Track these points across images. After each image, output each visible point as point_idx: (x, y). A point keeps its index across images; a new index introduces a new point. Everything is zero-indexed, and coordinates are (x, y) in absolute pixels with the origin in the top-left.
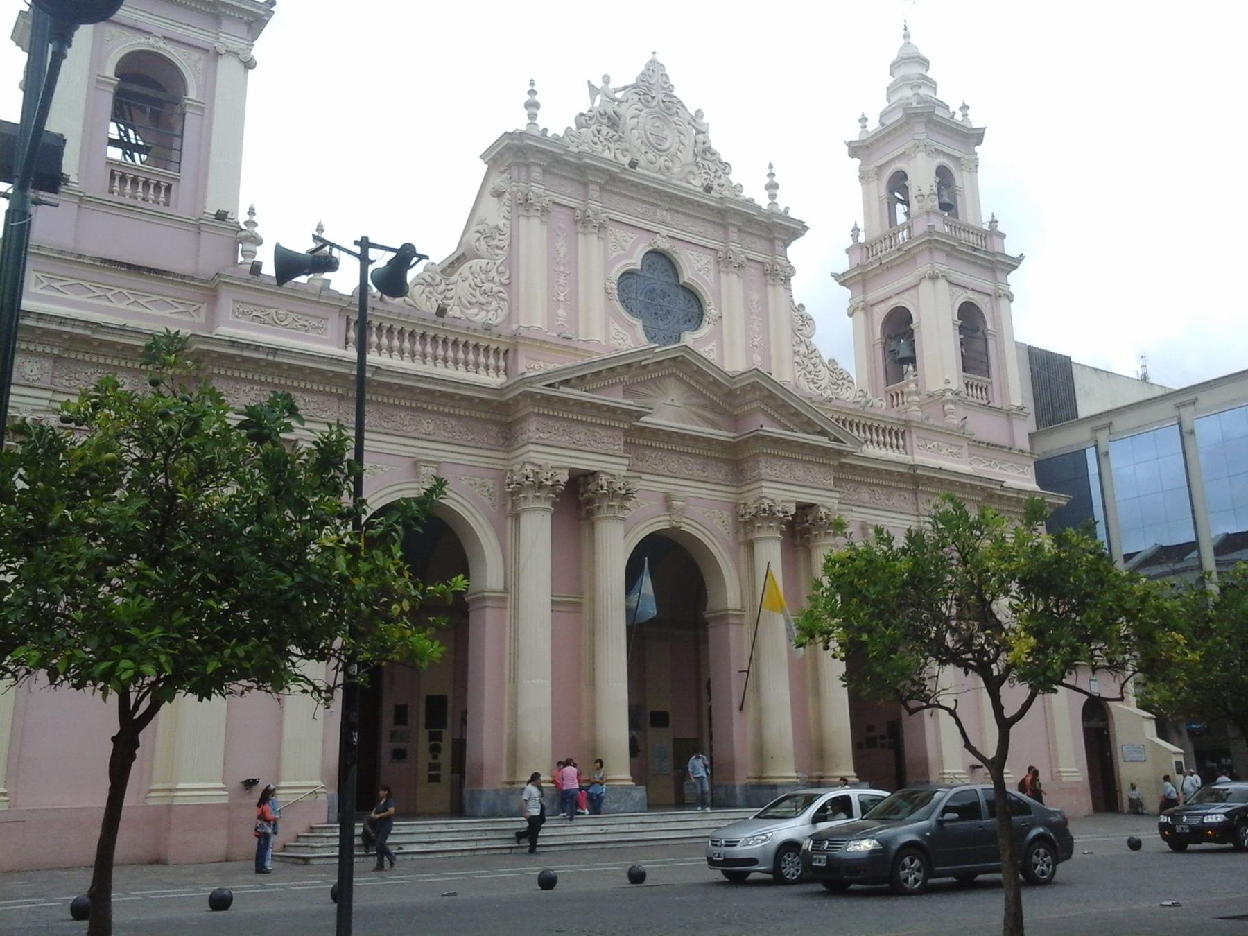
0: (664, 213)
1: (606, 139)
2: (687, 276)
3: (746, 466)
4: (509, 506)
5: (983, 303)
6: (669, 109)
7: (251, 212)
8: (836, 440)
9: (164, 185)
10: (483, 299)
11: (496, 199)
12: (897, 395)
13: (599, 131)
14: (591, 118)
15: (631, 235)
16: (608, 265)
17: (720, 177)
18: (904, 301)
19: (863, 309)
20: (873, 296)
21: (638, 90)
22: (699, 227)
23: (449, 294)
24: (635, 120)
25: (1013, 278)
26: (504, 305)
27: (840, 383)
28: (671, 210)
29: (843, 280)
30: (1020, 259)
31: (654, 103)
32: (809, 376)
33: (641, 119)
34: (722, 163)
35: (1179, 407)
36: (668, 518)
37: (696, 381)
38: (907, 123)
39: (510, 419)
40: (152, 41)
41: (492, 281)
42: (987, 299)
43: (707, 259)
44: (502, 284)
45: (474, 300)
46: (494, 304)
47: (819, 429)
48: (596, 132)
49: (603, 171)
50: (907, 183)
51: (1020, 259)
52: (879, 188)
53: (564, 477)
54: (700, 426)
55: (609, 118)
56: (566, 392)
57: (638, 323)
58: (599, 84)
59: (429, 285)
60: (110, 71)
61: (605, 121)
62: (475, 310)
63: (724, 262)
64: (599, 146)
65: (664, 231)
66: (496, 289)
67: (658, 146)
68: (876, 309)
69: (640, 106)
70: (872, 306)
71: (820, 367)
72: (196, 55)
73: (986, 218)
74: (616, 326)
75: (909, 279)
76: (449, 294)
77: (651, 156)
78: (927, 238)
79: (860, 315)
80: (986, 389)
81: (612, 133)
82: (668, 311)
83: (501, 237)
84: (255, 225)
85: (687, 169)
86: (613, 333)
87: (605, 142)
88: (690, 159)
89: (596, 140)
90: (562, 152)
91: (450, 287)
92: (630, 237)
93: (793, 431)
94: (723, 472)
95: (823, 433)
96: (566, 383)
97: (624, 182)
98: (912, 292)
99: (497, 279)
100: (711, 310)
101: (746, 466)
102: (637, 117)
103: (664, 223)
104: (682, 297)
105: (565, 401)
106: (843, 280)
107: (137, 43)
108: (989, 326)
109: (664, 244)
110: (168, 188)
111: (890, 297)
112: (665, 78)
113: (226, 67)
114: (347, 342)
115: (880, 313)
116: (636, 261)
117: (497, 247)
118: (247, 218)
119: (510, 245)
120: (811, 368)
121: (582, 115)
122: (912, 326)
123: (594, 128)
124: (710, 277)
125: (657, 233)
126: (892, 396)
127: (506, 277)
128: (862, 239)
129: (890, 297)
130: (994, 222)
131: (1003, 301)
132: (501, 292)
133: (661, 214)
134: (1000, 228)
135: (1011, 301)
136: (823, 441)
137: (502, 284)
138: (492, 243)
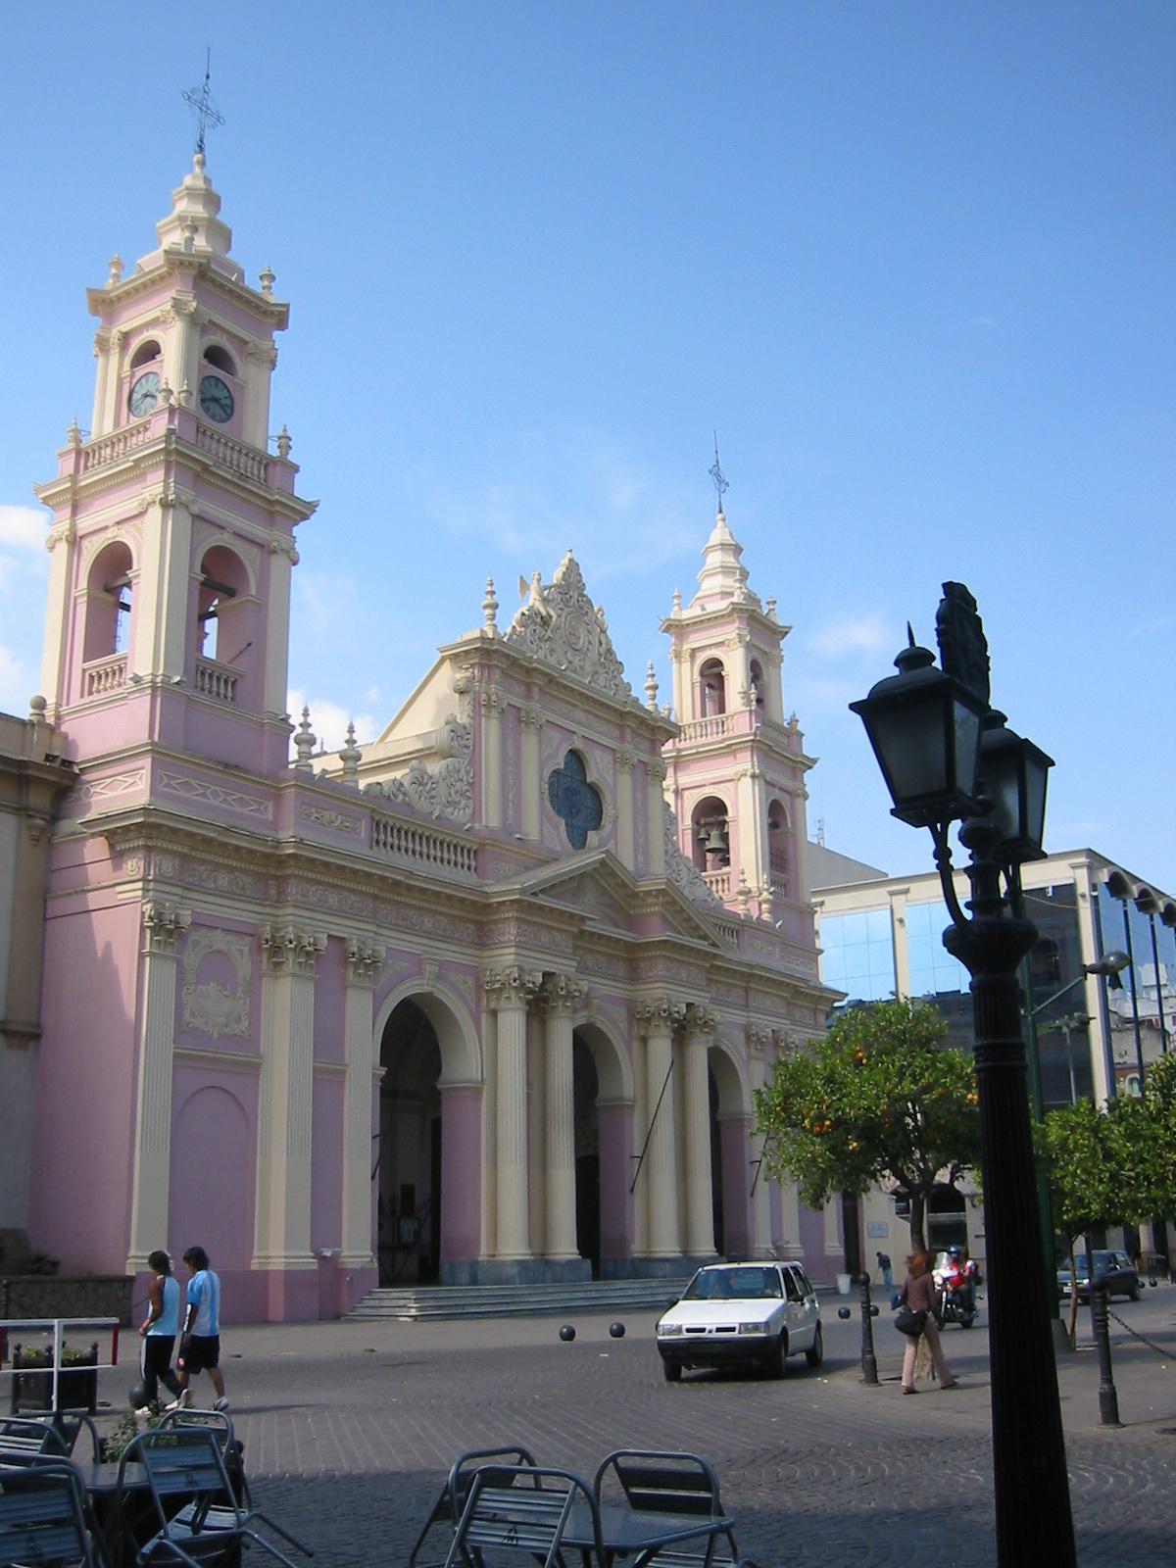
3: (642, 965)
4: (484, 1002)
5: (784, 800)
6: (581, 608)
7: (306, 714)
8: (714, 945)
10: (457, 798)
11: (457, 695)
13: (534, 631)
16: (542, 765)
17: (616, 677)
18: (721, 793)
22: (604, 727)
23: (433, 793)
25: (808, 776)
30: (815, 761)
34: (617, 662)
35: (892, 894)
37: (607, 882)
38: (730, 615)
39: (484, 919)
40: (226, 536)
42: (788, 797)
45: (450, 800)
47: (702, 933)
49: (546, 675)
50: (723, 673)
51: (815, 761)
54: (606, 925)
55: (542, 618)
56: (543, 900)
59: (420, 784)
61: (539, 620)
62: (450, 810)
65: (582, 731)
71: (682, 867)
72: (255, 551)
73: (787, 716)
76: (433, 793)
78: (752, 738)
83: (468, 736)
84: (310, 725)
88: (596, 658)
90: (521, 657)
91: (434, 786)
92: (556, 735)
93: (681, 934)
95: (705, 937)
97: (558, 684)
100: (608, 811)
101: (642, 965)
103: (579, 723)
105: (541, 908)
108: (789, 825)
109: (579, 744)
111: (704, 785)
112: (579, 578)
113: (277, 562)
118: (301, 720)
119: (474, 745)
120: (675, 867)
125: (575, 733)
127: (471, 775)
129: (704, 785)
130: (794, 721)
131: (799, 801)
132: (467, 791)
133: (579, 715)
134: (799, 727)
135: (806, 799)
136: (703, 945)
138: (461, 743)
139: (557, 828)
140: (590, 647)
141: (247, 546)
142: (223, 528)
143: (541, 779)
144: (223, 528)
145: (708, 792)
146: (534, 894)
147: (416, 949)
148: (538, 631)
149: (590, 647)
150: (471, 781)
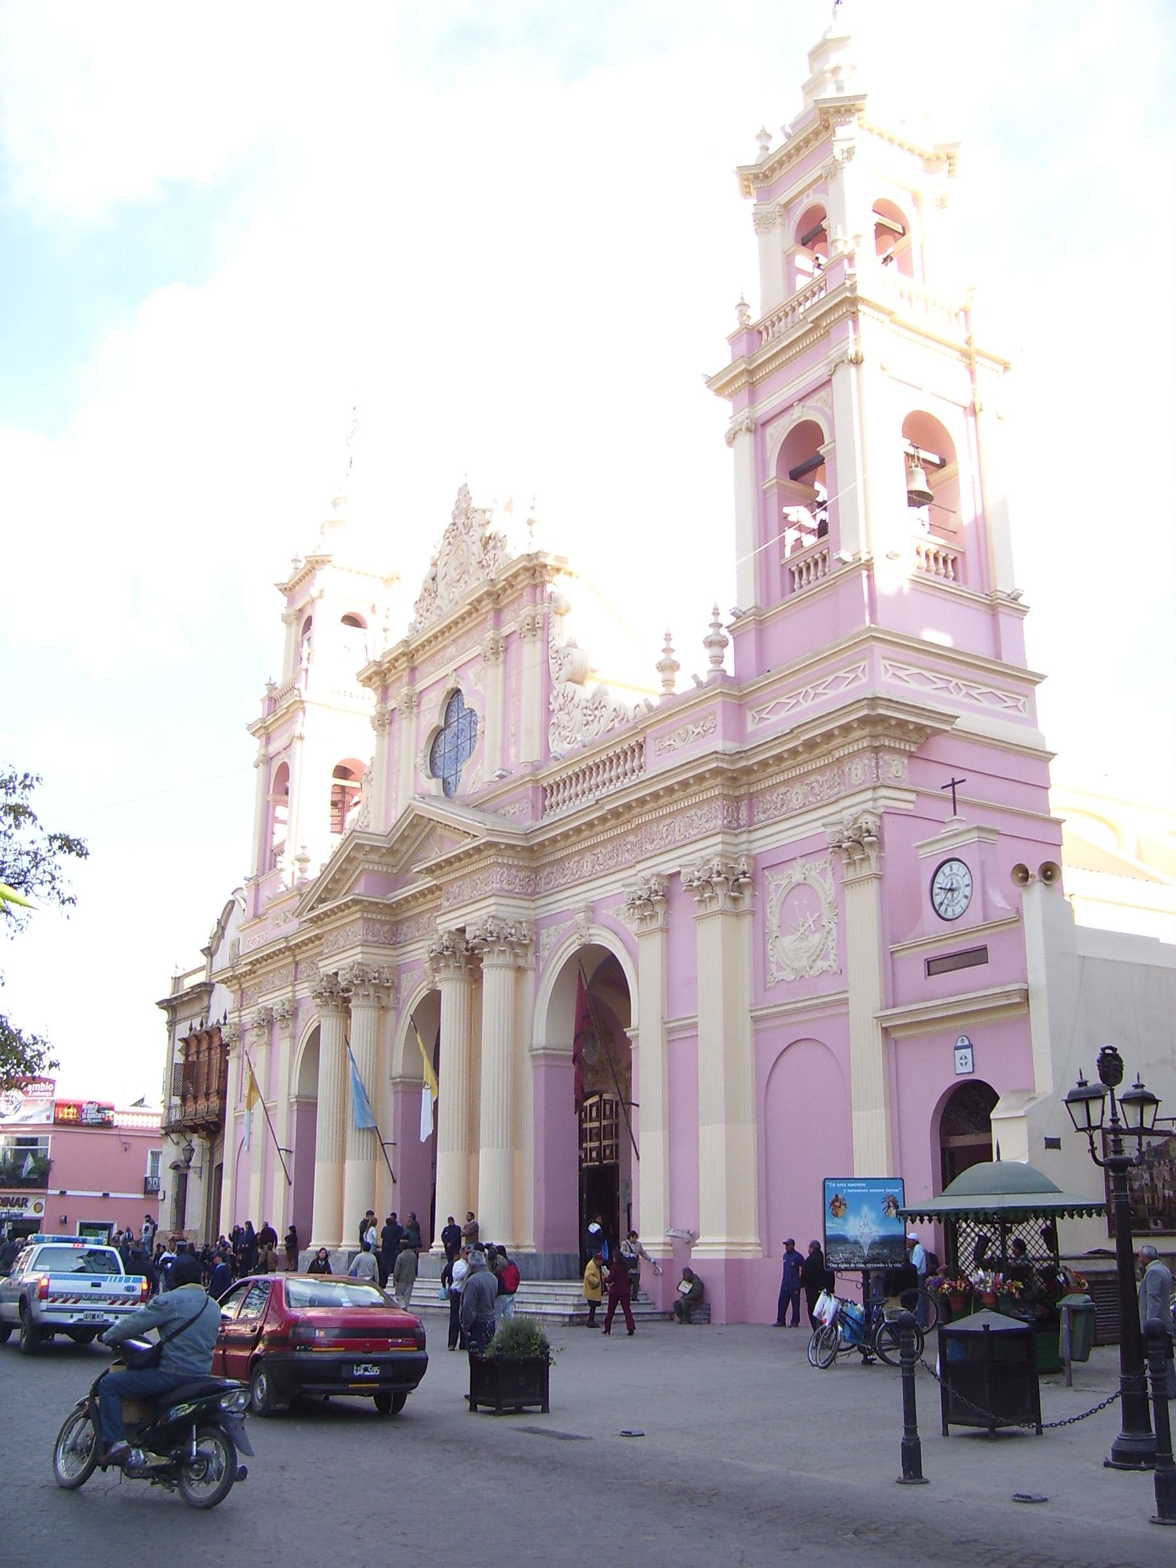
12: (801, 572)
19: (749, 430)
20: (767, 405)
29: (721, 385)
52: (784, 235)
68: (770, 430)
70: (763, 425)
75: (817, 372)
79: (745, 440)
80: (953, 561)
98: (823, 393)
106: (721, 385)
115: (777, 434)
122: (822, 450)
126: (793, 573)
128: (755, 316)
145: (798, 415)
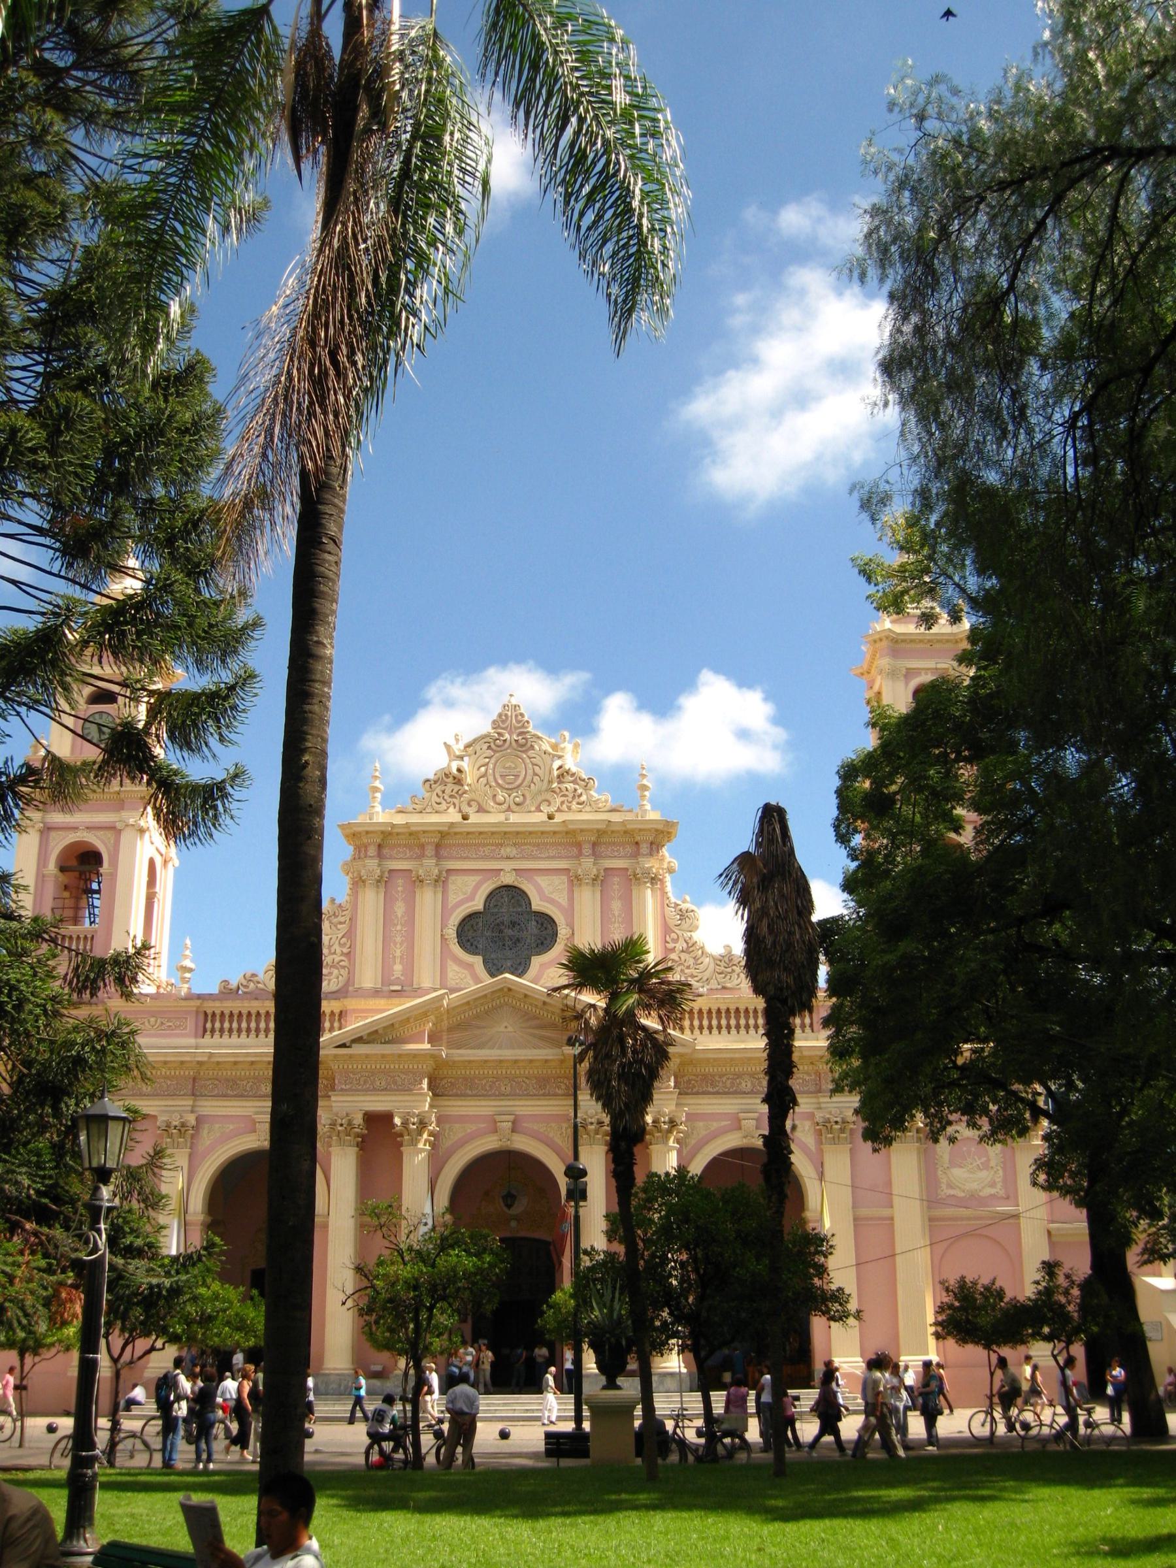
0: (508, 850)
1: (451, 796)
2: (537, 904)
9: (89, 936)
14: (435, 782)
15: (472, 878)
16: (445, 913)
17: (580, 795)
21: (488, 739)
24: (483, 769)
26: (344, 972)
27: (729, 970)
28: (515, 845)
31: (508, 743)
32: (687, 971)
33: (491, 766)
36: (495, 1138)
41: (335, 953)
43: (561, 881)
44: (343, 954)
46: (336, 972)
48: (440, 794)
53: (358, 1120)
54: (539, 1048)
57: (477, 961)
58: (451, 742)
60: (52, 866)
61: (450, 780)
63: (575, 880)
64: (444, 806)
65: (508, 866)
66: (337, 959)
67: (510, 786)
69: (490, 752)
72: (110, 834)
74: (456, 968)
77: (500, 798)
81: (456, 788)
82: (518, 940)
85: (540, 799)
86: (450, 975)
87: (449, 800)
89: (438, 800)
92: (472, 880)
94: (563, 1087)
96: (359, 1040)
99: (338, 951)
102: (487, 764)
103: (508, 858)
104: (534, 923)
107: (72, 838)
109: (508, 879)
110: (92, 937)
114: (205, 1031)
116: (478, 904)
117: (341, 923)
120: (691, 962)
121: (428, 780)
123: (438, 790)
124: (563, 900)
137: (343, 954)
139: (470, 967)
140: (536, 779)
141: (101, 833)
142: (77, 828)
143: (444, 926)
144: (75, 829)
146: (343, 1046)
147: (248, 1112)
148: (448, 791)
149: (536, 779)
150: (345, 950)
